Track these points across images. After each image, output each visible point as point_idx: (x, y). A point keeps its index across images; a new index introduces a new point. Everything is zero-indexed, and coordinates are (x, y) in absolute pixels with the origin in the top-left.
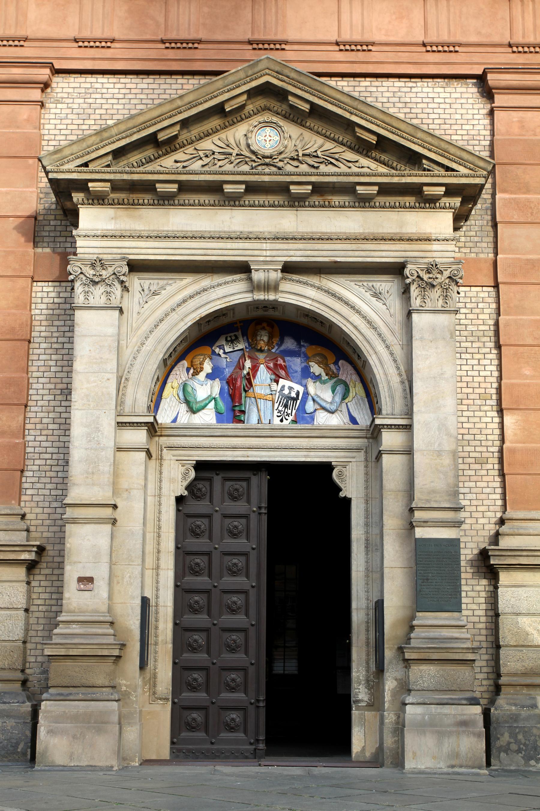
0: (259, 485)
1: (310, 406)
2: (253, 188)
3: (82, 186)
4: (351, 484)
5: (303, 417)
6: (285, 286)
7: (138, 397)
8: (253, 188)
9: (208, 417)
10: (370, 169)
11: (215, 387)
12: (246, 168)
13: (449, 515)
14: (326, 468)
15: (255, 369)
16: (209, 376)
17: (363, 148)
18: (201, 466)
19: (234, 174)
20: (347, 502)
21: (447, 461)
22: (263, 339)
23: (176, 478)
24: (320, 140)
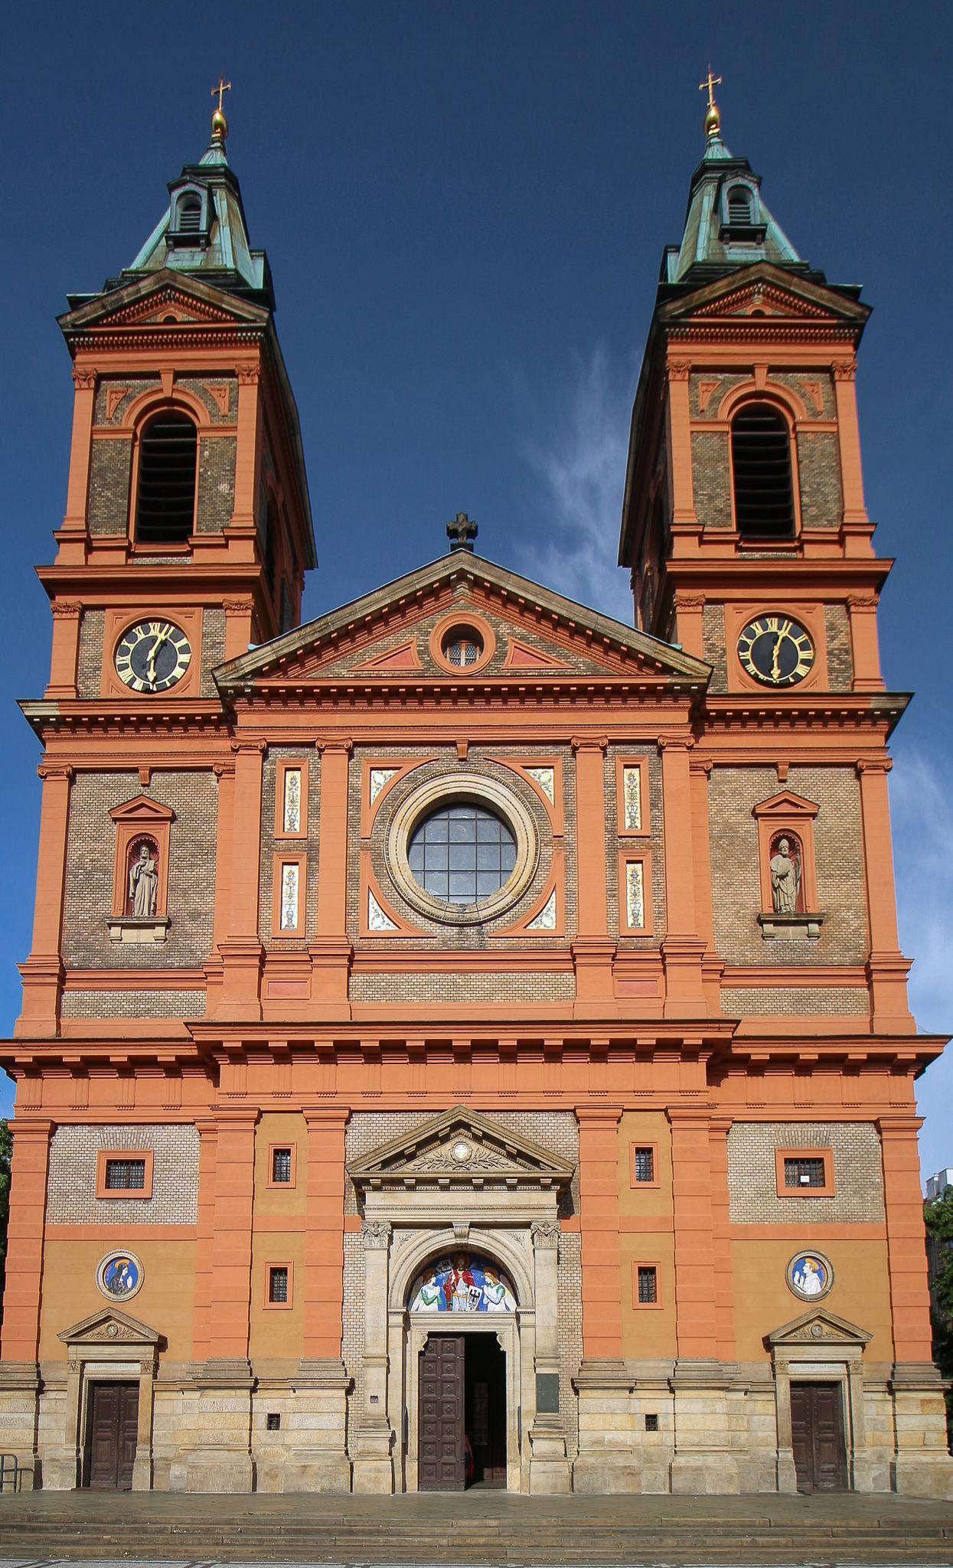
0: (460, 1341)
1: (485, 1301)
2: (455, 1181)
3: (366, 1181)
4: (507, 1343)
5: (482, 1307)
6: (472, 1235)
7: (398, 1297)
8: (455, 1181)
9: (434, 1306)
10: (516, 1169)
11: (436, 1291)
12: (450, 1169)
13: (553, 1361)
14: (494, 1335)
15: (457, 1280)
16: (435, 1285)
17: (511, 1156)
18: (431, 1335)
19: (444, 1172)
20: (504, 1353)
21: (552, 1331)
22: (462, 1262)
23: (417, 1341)
24: (488, 1152)
